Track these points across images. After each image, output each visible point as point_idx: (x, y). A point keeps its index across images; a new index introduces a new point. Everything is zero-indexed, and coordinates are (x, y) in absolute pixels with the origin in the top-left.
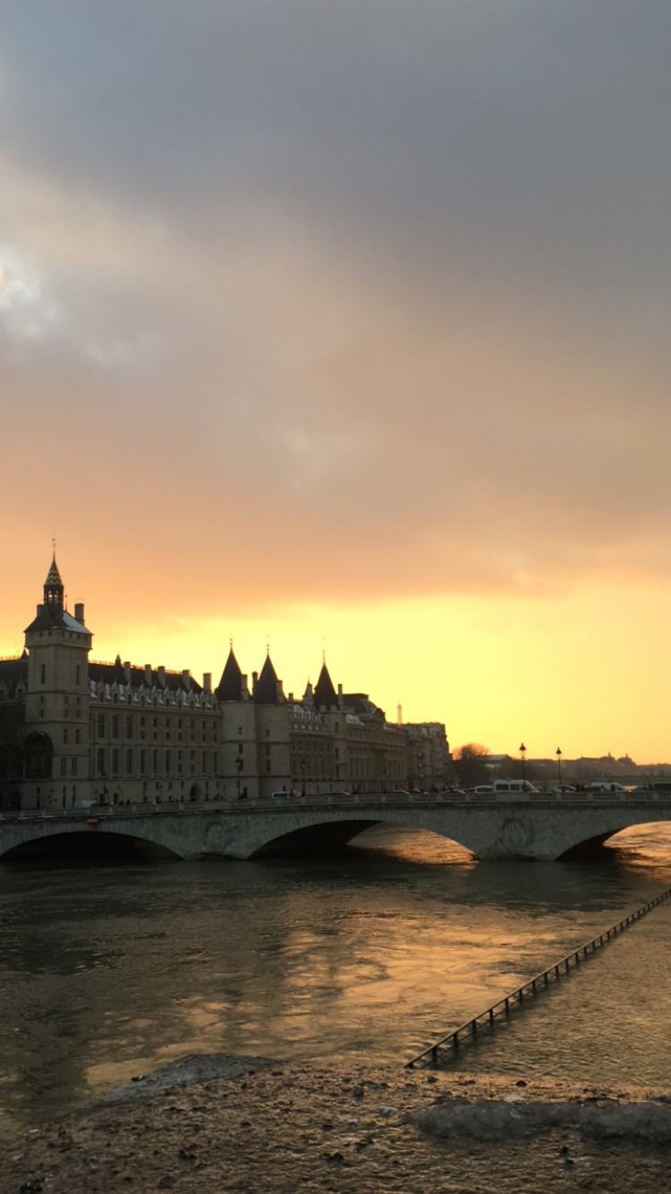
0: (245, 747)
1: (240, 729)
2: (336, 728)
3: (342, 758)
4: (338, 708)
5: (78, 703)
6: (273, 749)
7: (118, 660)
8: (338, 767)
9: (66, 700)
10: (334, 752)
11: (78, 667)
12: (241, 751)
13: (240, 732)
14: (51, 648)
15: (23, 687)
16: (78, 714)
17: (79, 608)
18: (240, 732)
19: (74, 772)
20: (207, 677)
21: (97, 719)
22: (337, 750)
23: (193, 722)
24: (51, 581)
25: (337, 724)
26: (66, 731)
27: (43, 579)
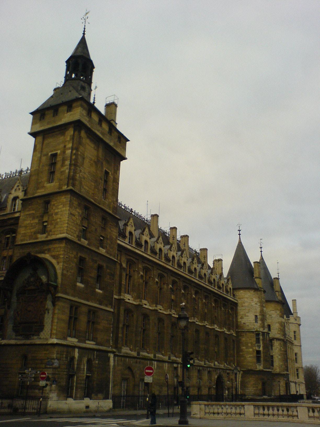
0: (261, 337)
1: (256, 316)
2: (295, 336)
4: (296, 320)
12: (258, 341)
15: (21, 194)
22: (296, 354)
26: (82, 260)
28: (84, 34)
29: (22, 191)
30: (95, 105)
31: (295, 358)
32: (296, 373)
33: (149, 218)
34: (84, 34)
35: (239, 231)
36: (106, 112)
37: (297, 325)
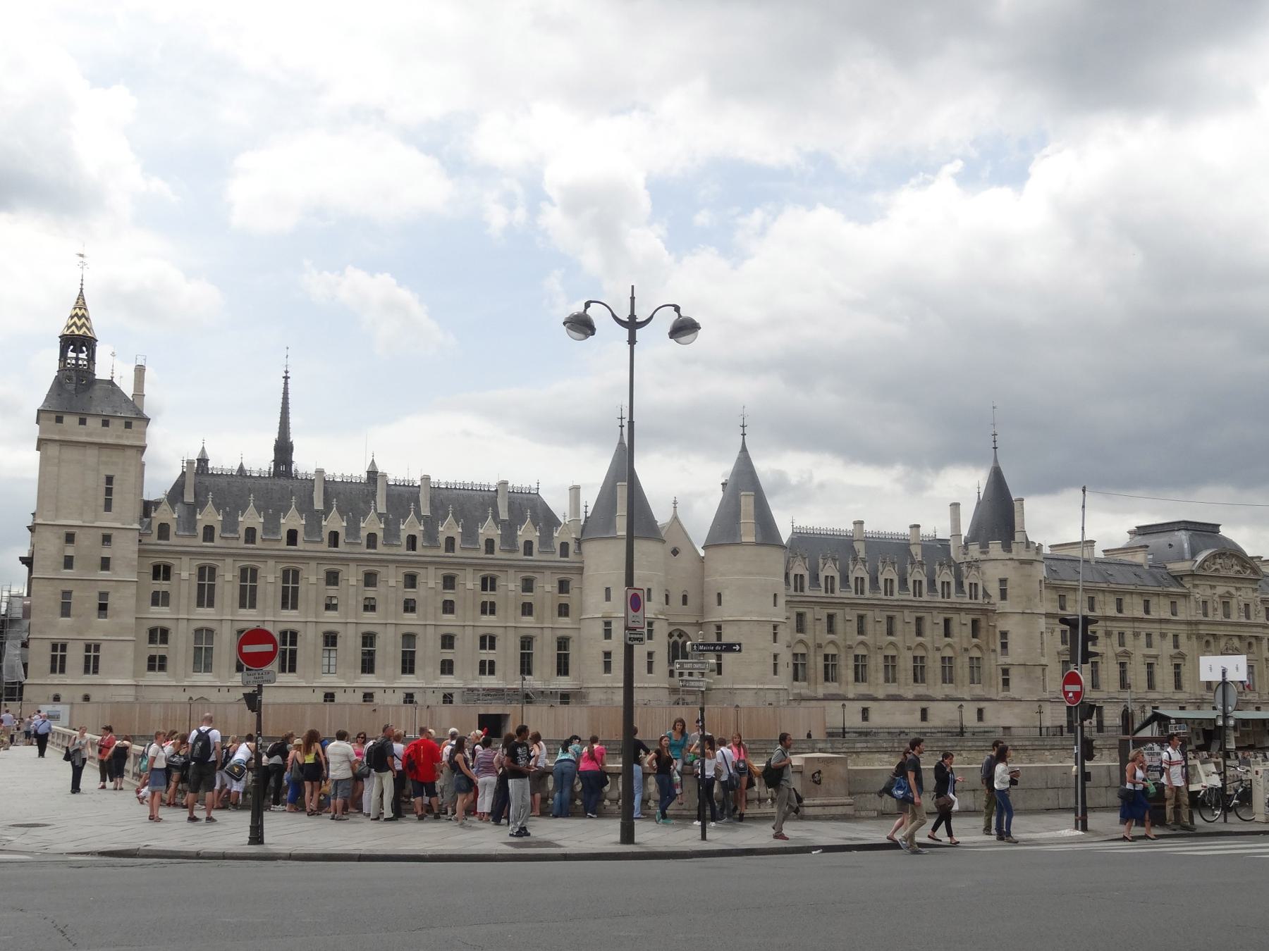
1: (608, 590)
3: (1017, 652)
7: (373, 475)
8: (1005, 672)
9: (70, 538)
11: (109, 480)
12: (608, 634)
13: (608, 598)
16: (105, 564)
17: (140, 371)
18: (608, 598)
20: (575, 490)
22: (1004, 634)
24: (74, 328)
25: (1003, 581)
26: (67, 594)
27: (59, 325)
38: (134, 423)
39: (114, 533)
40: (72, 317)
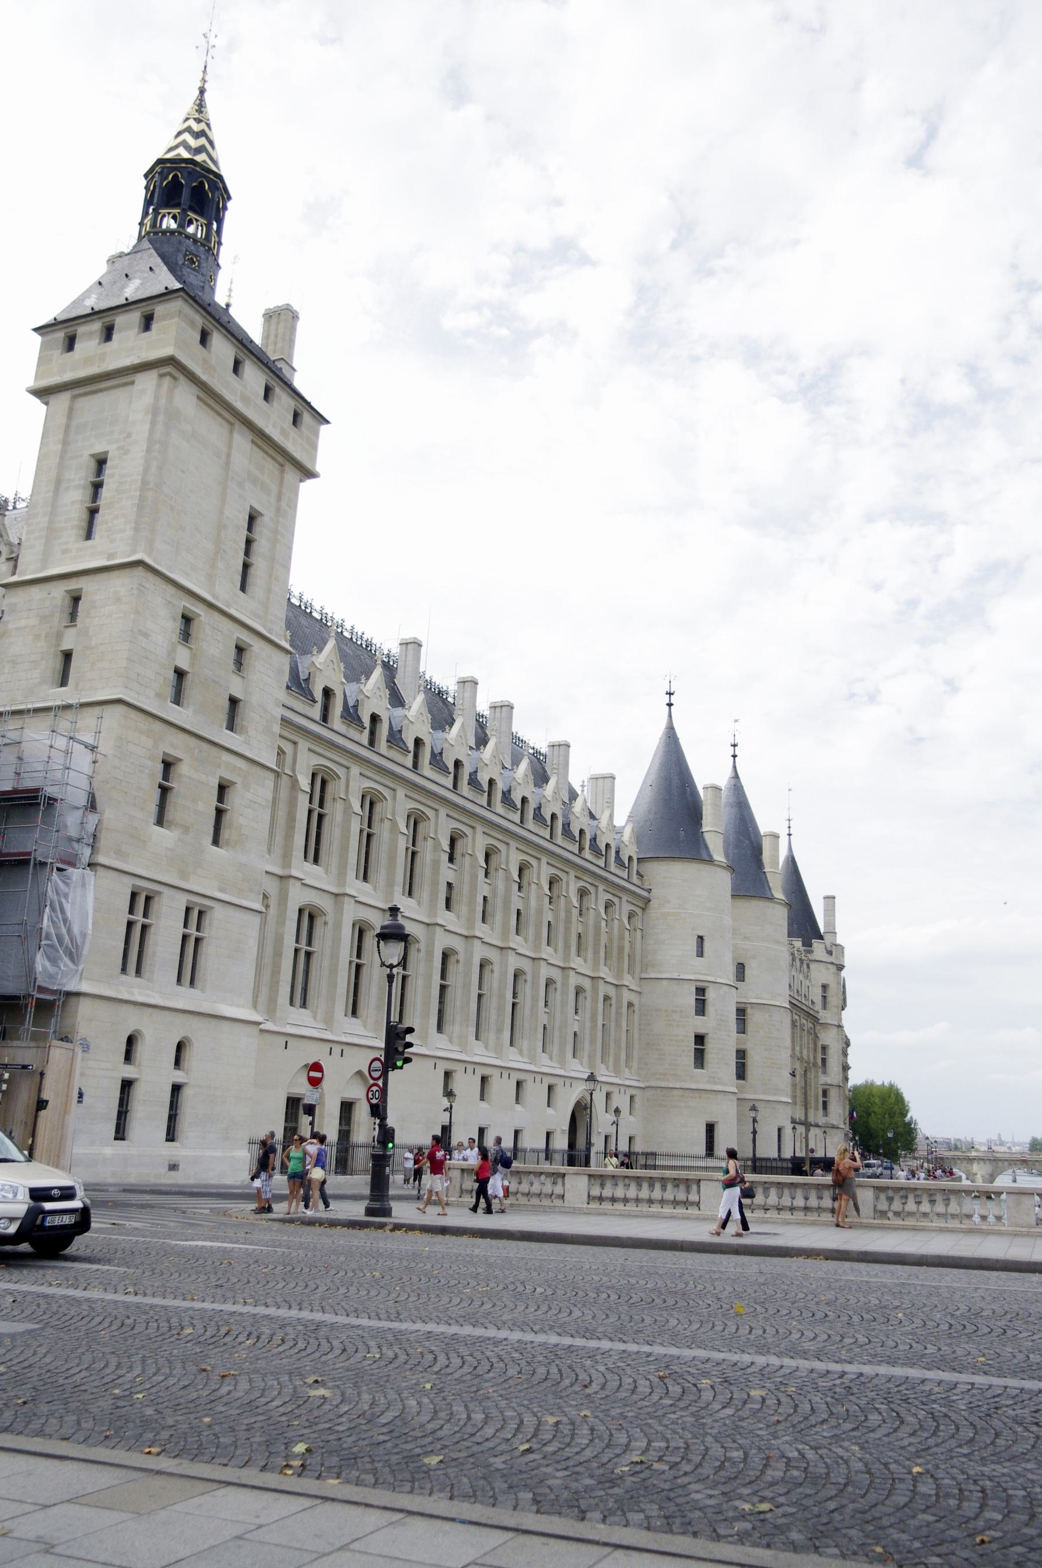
0: (710, 995)
2: (824, 997)
4: (830, 953)
5: (239, 664)
6: (754, 1017)
8: (825, 1093)
10: (820, 1056)
12: (701, 1007)
13: (700, 953)
14: (147, 381)
18: (700, 953)
19: (189, 969)
21: (304, 783)
22: (824, 1048)
23: (583, 893)
26: (168, 765)
28: (202, 91)
29: (8, 559)
30: (232, 311)
31: (820, 1064)
32: (821, 1099)
33: (395, 650)
34: (202, 91)
35: (670, 694)
36: (266, 336)
37: (833, 969)
38: (306, 418)
39: (257, 646)
40: (179, 134)
